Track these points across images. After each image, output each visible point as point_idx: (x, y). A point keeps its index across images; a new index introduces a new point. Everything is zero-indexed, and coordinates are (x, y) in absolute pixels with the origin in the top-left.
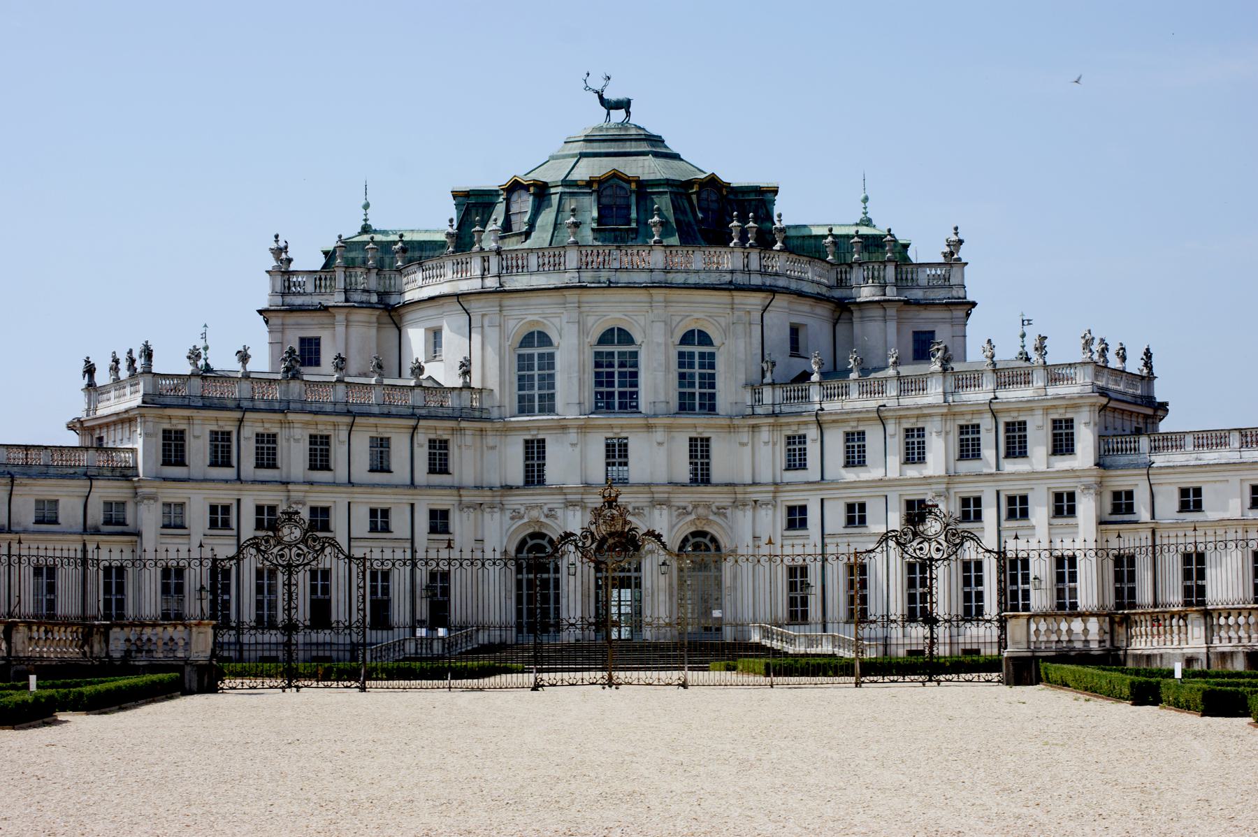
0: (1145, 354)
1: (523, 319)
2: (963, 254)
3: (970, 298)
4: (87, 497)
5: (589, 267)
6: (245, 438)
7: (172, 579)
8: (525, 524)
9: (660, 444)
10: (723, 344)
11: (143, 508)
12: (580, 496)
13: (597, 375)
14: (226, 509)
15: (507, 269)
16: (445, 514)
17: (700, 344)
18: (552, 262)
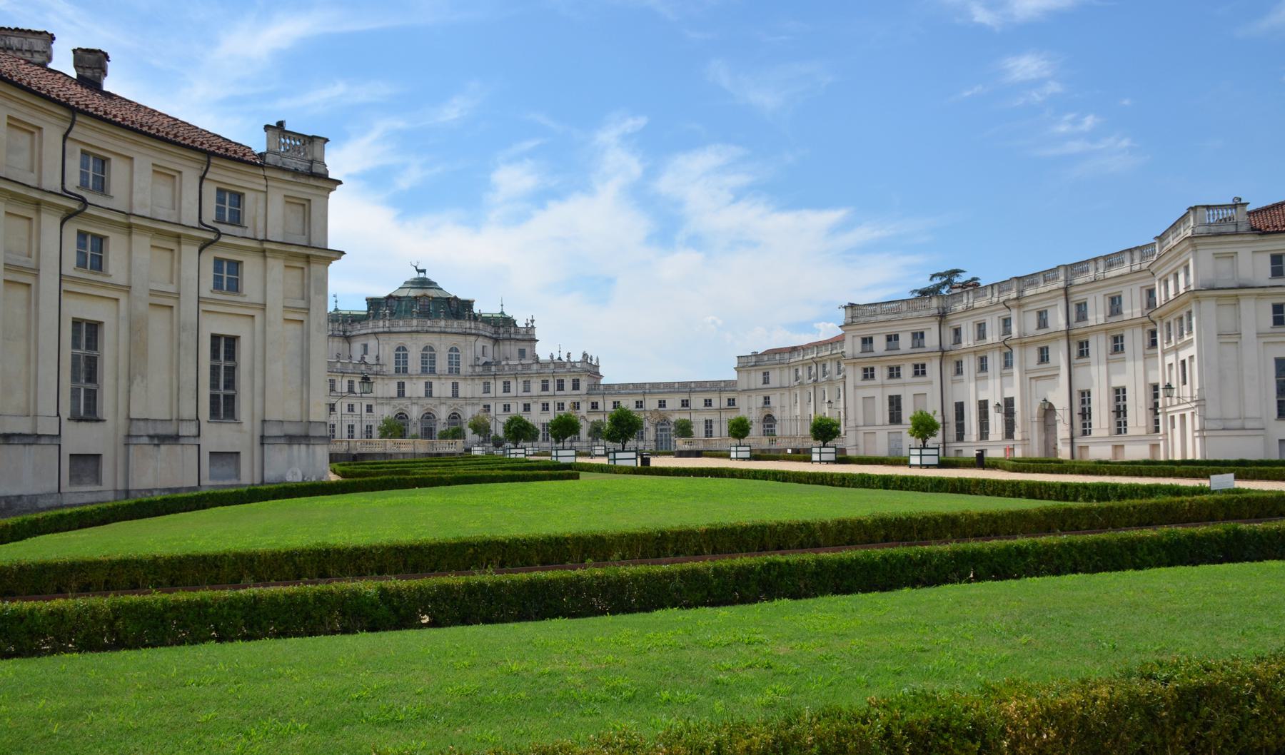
2: (535, 324)
16: (371, 406)
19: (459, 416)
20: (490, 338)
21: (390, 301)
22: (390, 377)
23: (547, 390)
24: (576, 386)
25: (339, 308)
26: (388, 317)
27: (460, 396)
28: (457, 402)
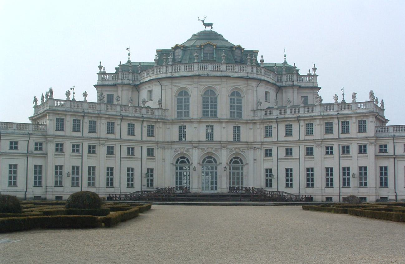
0: (382, 102)
2: (317, 73)
3: (318, 86)
4: (29, 141)
5: (201, 69)
6: (86, 122)
7: (59, 169)
8: (178, 154)
9: (224, 128)
11: (49, 144)
12: (197, 145)
13: (204, 105)
14: (78, 146)
15: (174, 70)
16: (152, 150)
17: (238, 96)
18: (189, 68)
19: (241, 160)
20: (274, 84)
21: (176, 51)
22: (173, 122)
23: (331, 133)
24: (362, 128)
26: (170, 63)
27: (242, 140)
28: (239, 146)
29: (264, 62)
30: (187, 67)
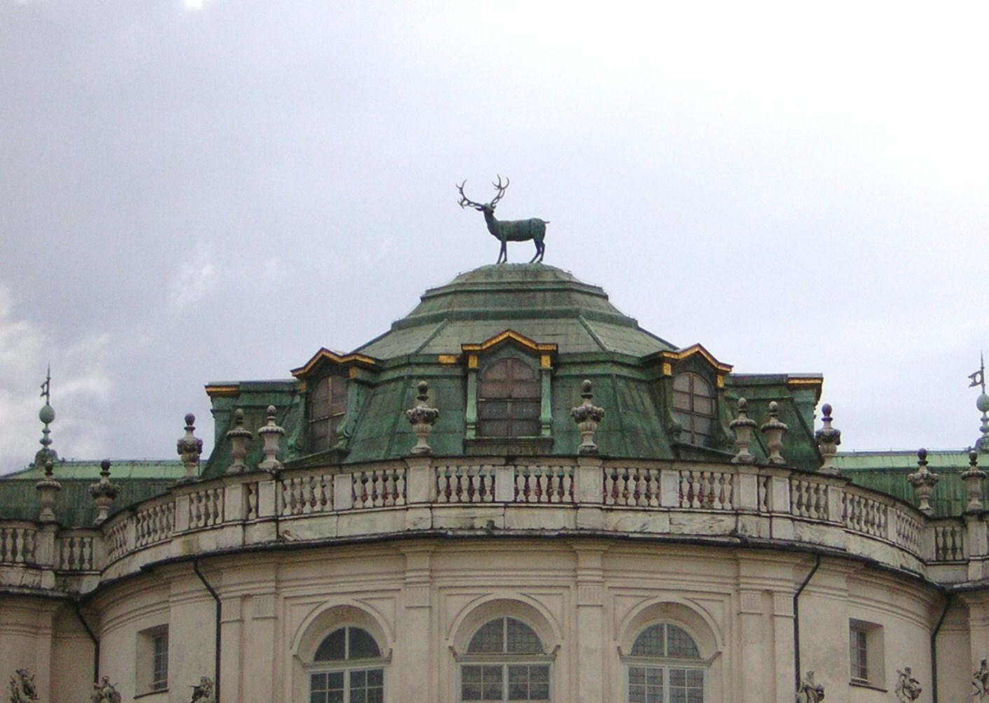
1: (321, 604)
5: (454, 498)
10: (720, 653)
18: (379, 491)
20: (902, 579)
25: (60, 449)
29: (838, 443)
30: (369, 485)
